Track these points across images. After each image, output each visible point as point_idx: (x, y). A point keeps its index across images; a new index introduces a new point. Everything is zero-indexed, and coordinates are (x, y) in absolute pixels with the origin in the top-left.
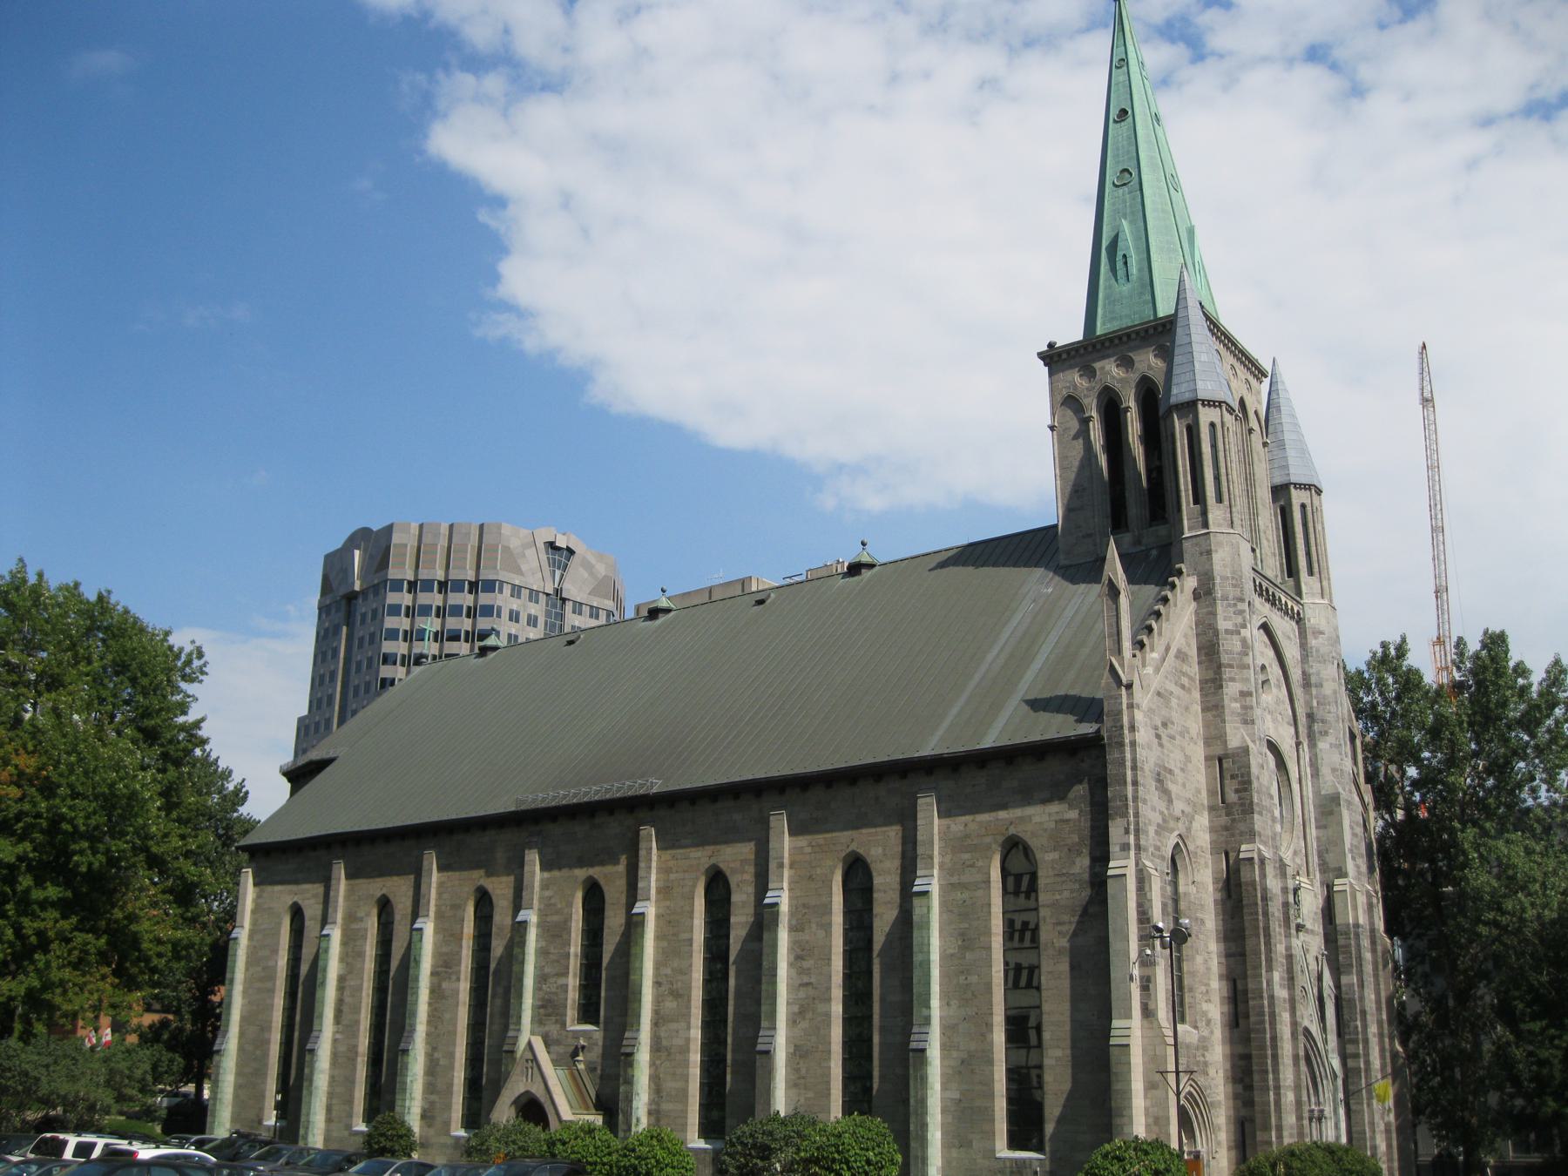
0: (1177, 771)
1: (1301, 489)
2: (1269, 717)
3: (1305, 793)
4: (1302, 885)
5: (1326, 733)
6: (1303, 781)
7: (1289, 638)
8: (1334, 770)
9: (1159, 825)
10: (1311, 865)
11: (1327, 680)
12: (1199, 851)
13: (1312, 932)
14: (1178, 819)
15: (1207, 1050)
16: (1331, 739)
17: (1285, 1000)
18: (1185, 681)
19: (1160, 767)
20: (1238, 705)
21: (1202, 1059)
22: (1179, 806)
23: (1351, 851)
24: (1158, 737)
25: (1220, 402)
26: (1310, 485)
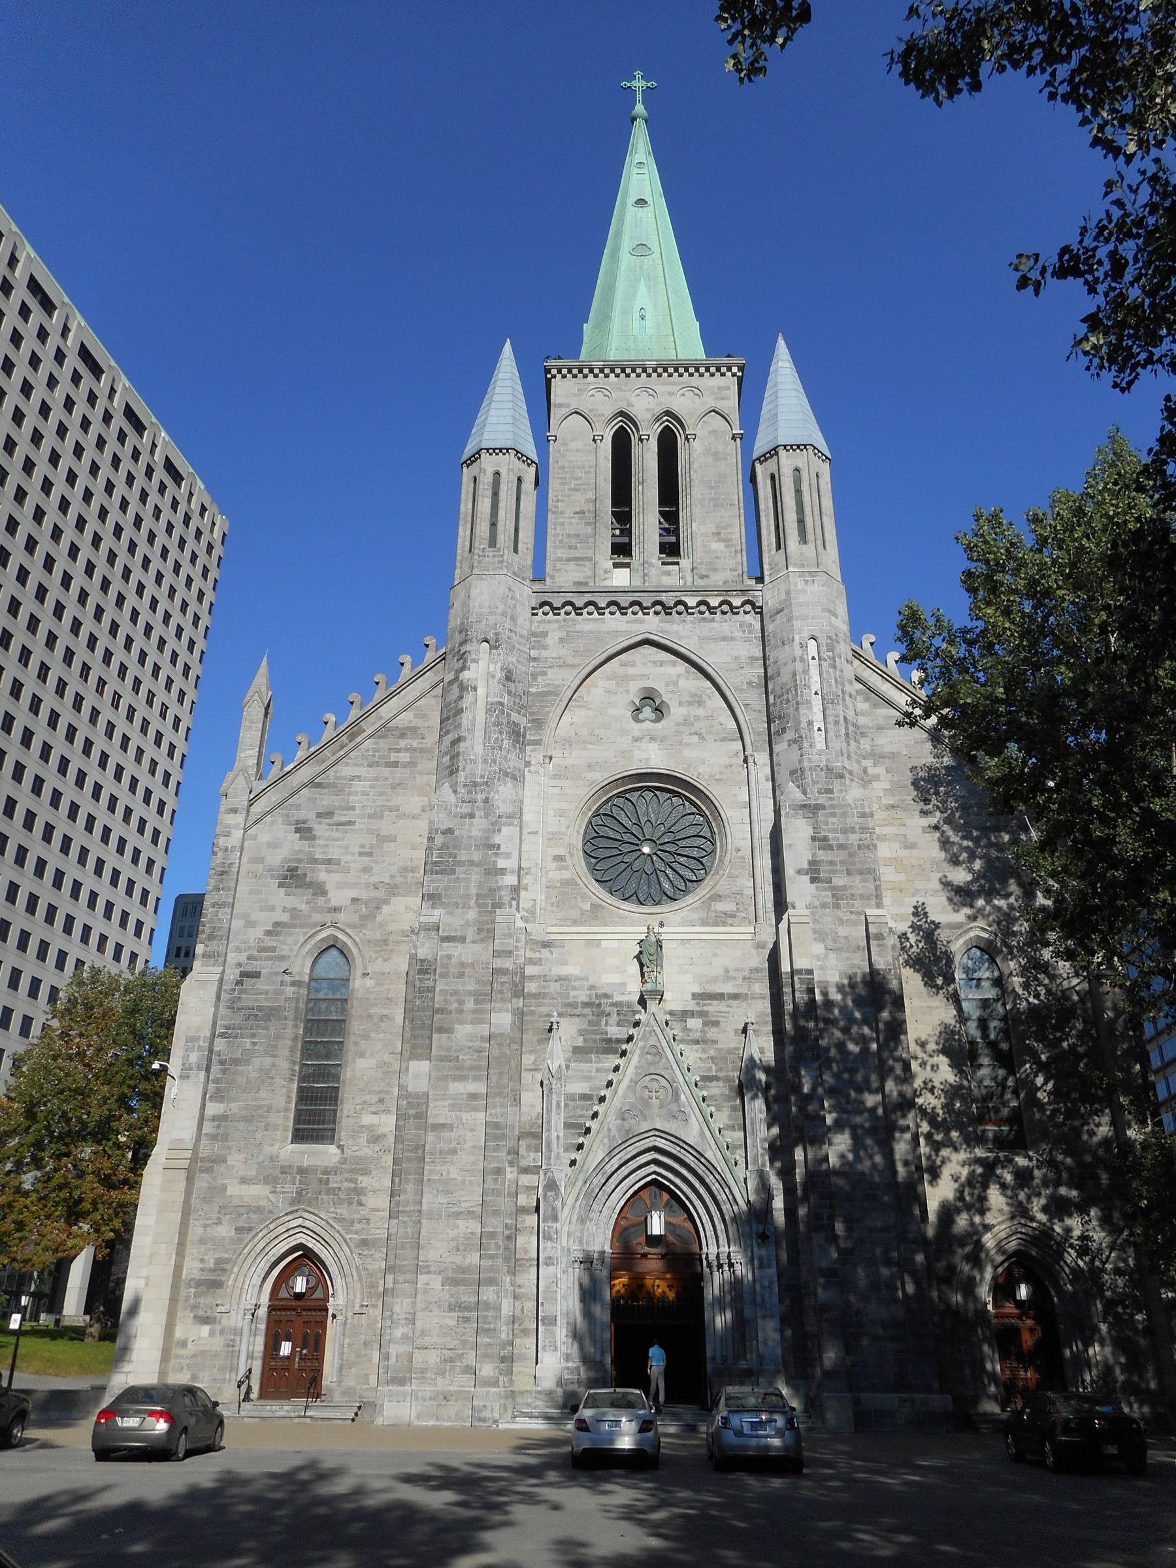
0: (344, 858)
1: (766, 459)
2: (654, 746)
3: (755, 817)
4: (663, 937)
5: (784, 730)
6: (754, 804)
7: (724, 639)
8: (793, 772)
9: (277, 924)
10: (760, 906)
11: (785, 664)
12: (392, 938)
13: (736, 997)
14: (336, 910)
15: (365, 1172)
16: (789, 735)
17: (473, 1097)
18: (404, 757)
19: (300, 861)
20: (448, 758)
21: (347, 1185)
22: (338, 896)
23: (814, 872)
24: (297, 830)
25: (478, 453)
26: (774, 449)
